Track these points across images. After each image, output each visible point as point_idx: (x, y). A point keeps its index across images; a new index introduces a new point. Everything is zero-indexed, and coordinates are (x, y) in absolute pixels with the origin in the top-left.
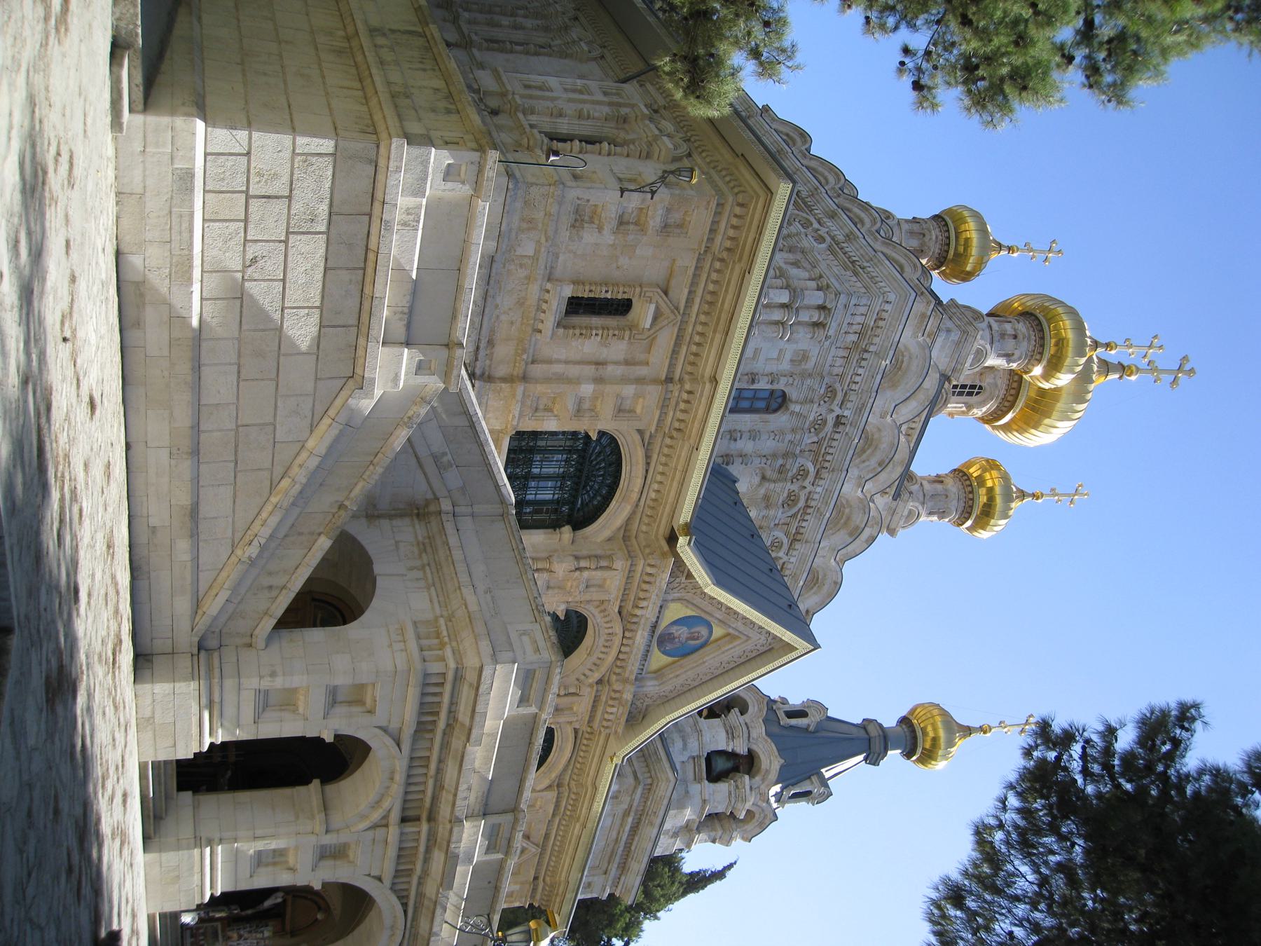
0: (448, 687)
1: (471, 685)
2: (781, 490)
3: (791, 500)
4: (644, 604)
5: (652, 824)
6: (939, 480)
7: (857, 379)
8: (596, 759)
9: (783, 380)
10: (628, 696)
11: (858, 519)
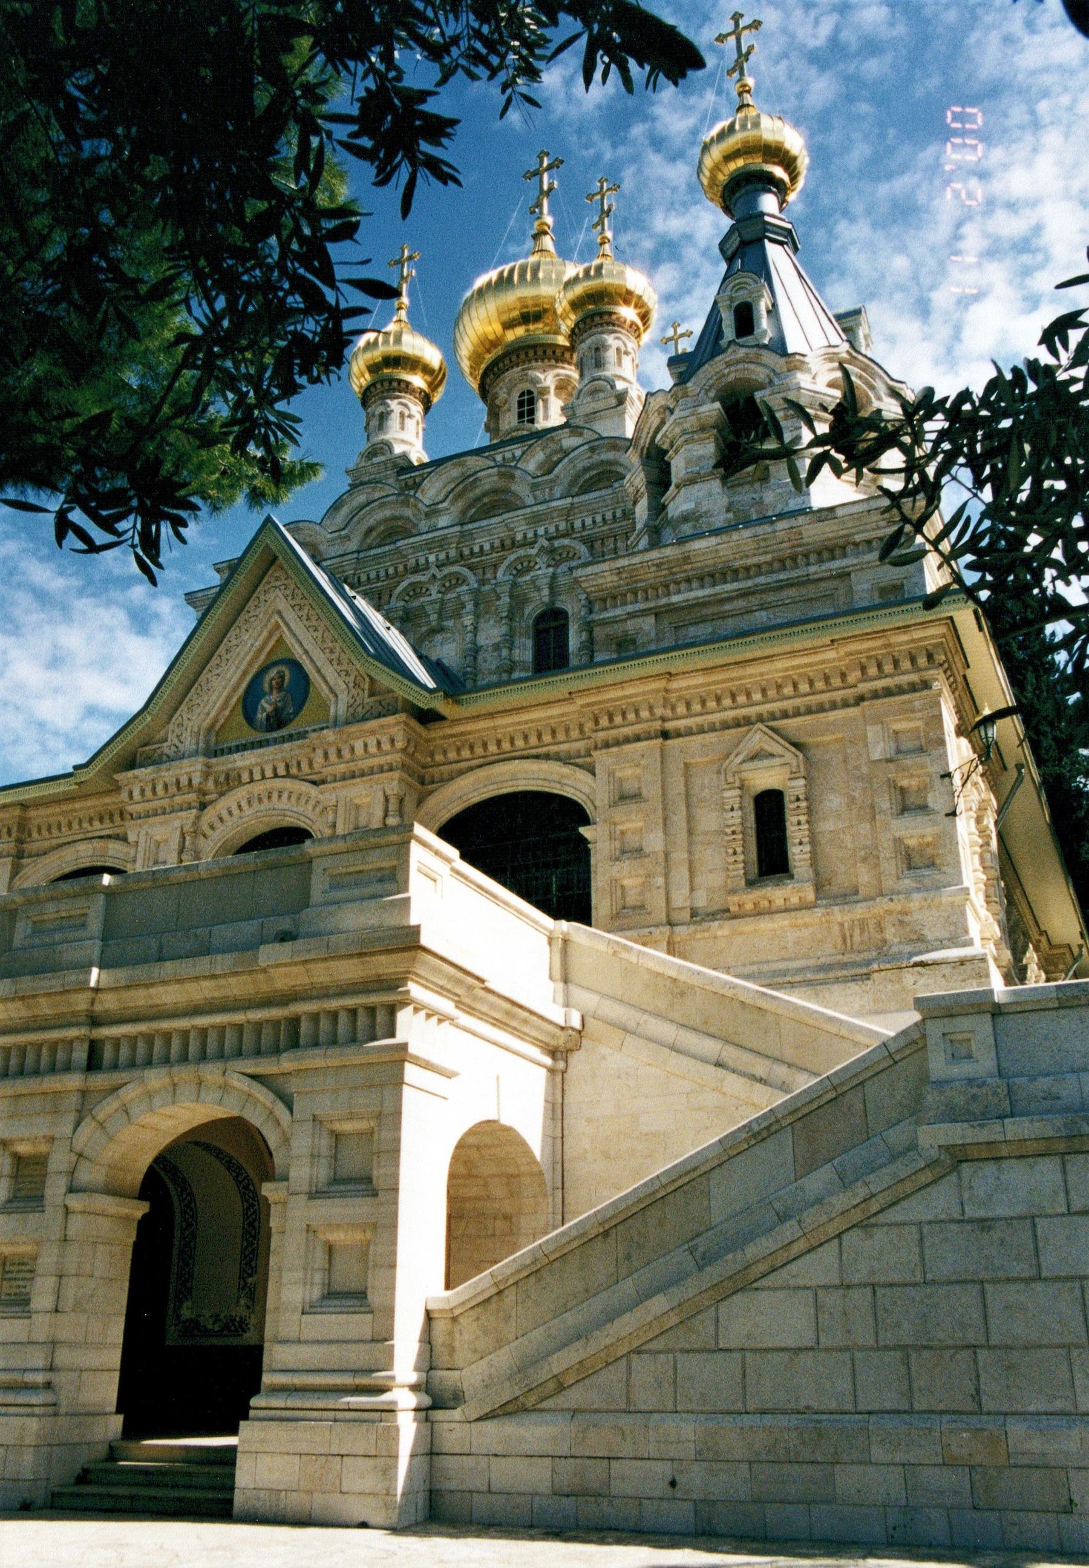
4: (184, 781)
5: (686, 559)
8: (525, 717)
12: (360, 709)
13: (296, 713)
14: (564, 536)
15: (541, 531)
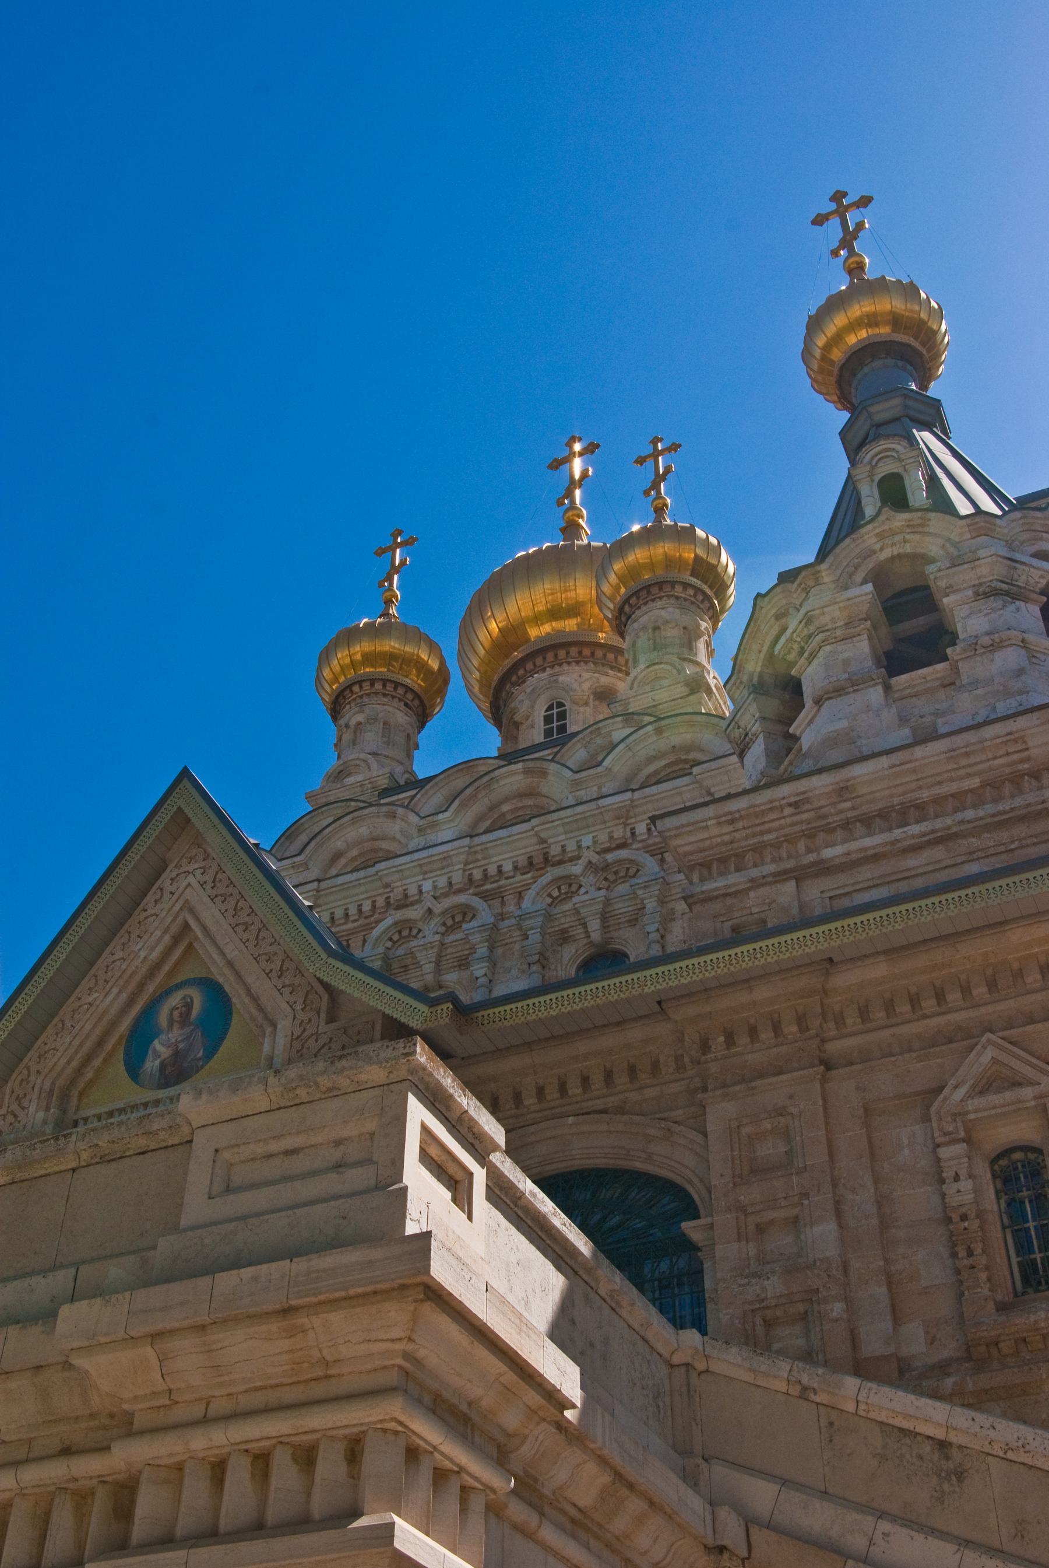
5: (843, 791)
12: (311, 1042)
13: (209, 1055)
14: (620, 847)
15: (587, 841)
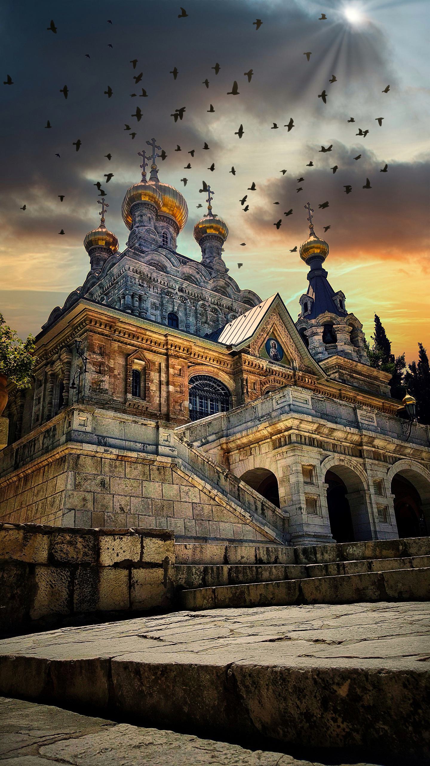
0: (302, 433)
1: (300, 423)
2: (210, 315)
3: (215, 311)
4: (261, 366)
6: (204, 251)
7: (162, 282)
9: (164, 313)
10: (300, 374)
11: (222, 283)
